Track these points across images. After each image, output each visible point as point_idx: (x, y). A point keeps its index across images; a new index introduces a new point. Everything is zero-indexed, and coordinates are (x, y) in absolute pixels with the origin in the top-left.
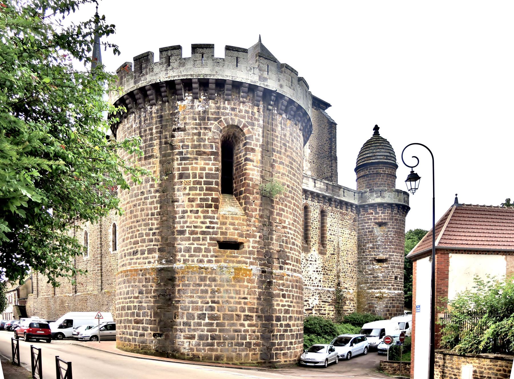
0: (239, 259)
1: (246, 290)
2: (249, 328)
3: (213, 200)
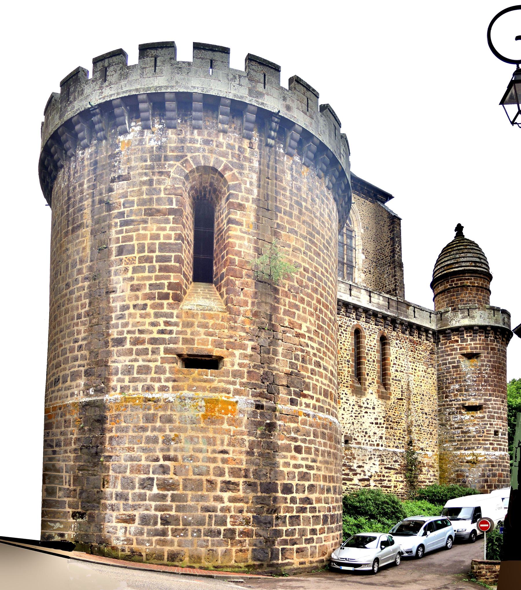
0: (215, 384)
1: (226, 437)
2: (232, 505)
3: (171, 286)
